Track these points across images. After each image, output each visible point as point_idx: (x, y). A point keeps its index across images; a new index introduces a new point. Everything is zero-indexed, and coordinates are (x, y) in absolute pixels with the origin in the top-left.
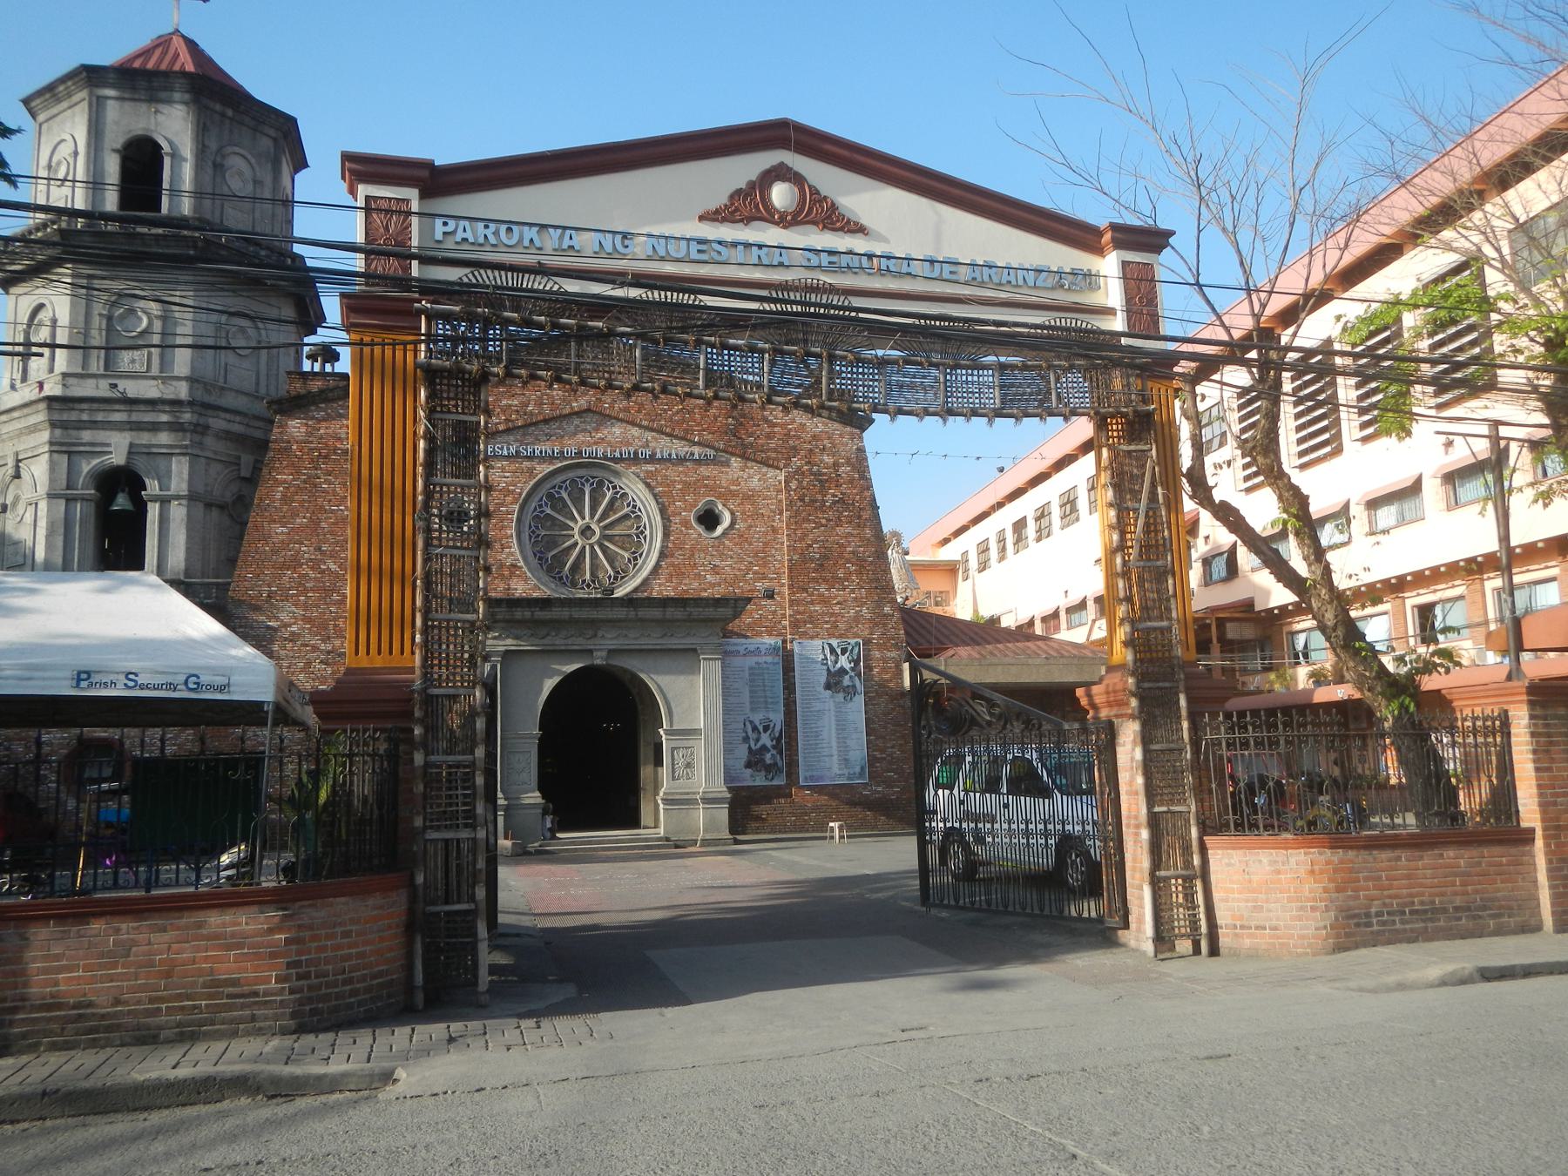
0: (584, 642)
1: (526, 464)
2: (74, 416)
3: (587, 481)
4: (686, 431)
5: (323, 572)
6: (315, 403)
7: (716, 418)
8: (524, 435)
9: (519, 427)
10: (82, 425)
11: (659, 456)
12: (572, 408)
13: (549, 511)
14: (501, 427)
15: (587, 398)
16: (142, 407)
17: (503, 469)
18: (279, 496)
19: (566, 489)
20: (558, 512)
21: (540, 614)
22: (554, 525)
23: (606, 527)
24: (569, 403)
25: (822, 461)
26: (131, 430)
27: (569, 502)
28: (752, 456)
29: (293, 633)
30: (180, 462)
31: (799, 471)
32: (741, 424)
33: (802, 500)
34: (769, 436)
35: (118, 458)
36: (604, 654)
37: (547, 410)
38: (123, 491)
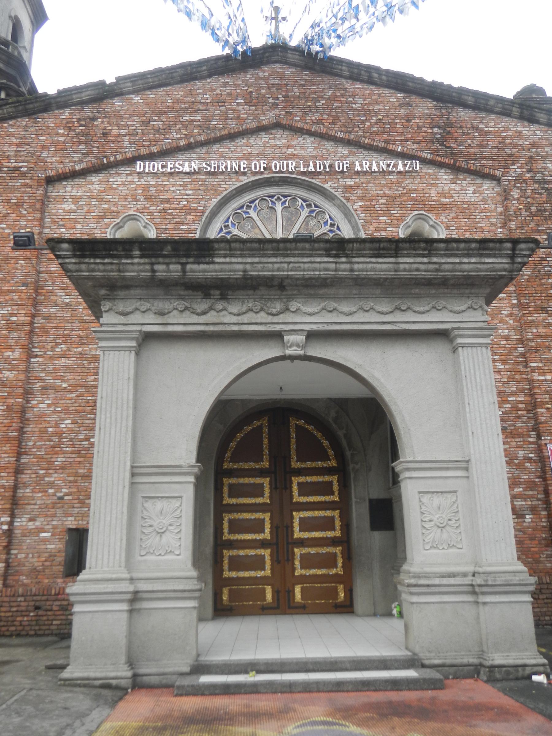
0: (270, 319)
1: (211, 180)
3: (279, 199)
4: (386, 141)
8: (207, 153)
11: (358, 168)
13: (235, 231)
14: (182, 143)
15: (277, 111)
17: (184, 186)
24: (256, 117)
25: (545, 168)
28: (464, 165)
31: (519, 180)
32: (449, 133)
33: (527, 208)
34: (482, 145)
36: (301, 338)
37: (233, 126)
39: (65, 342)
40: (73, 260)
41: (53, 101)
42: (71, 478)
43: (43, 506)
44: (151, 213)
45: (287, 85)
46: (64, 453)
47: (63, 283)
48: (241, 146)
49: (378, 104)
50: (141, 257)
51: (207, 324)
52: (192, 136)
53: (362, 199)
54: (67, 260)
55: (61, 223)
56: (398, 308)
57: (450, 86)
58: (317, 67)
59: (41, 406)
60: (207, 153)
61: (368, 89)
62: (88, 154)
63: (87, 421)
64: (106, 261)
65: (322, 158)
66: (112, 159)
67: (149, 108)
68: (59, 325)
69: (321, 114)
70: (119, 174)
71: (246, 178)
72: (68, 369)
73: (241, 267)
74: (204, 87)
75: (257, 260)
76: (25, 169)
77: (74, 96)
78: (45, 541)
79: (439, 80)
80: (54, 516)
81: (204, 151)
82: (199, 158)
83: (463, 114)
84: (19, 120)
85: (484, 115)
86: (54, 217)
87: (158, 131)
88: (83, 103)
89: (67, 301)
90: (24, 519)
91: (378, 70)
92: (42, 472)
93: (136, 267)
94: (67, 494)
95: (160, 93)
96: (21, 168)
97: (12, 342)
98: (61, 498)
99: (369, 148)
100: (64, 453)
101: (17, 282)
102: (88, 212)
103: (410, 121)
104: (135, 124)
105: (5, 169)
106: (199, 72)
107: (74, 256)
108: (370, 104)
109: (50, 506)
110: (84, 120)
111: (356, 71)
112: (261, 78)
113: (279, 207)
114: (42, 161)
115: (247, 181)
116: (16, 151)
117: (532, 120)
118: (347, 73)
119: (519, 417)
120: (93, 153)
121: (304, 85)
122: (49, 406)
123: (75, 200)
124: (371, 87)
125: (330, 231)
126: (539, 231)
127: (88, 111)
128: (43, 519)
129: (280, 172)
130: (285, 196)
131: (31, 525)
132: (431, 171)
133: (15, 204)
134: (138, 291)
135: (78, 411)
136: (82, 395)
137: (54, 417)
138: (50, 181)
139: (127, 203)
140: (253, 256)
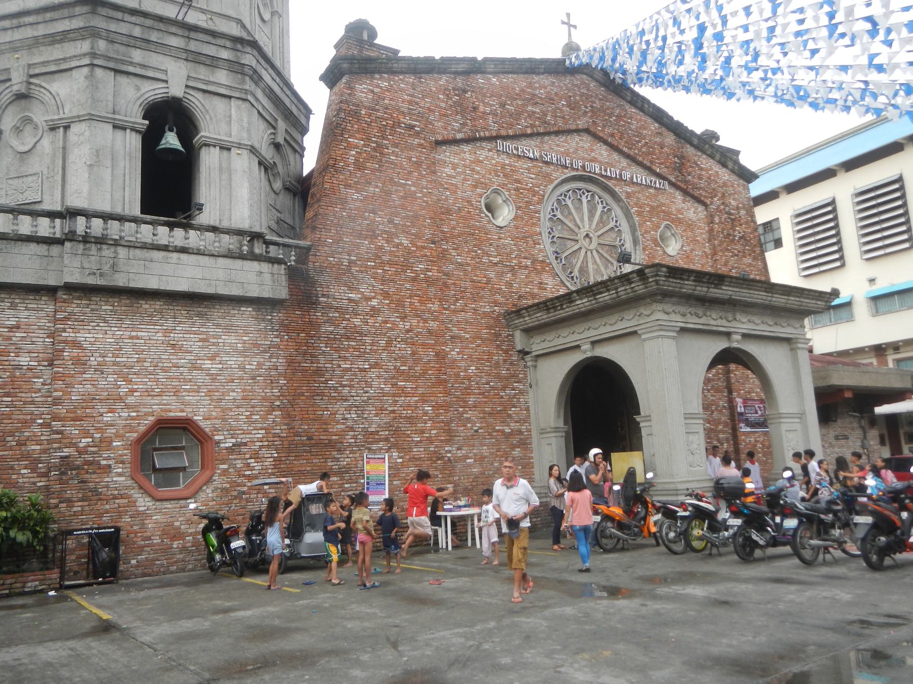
1: (545, 169)
2: (124, 28)
5: (397, 246)
6: (380, 72)
7: (668, 155)
8: (542, 142)
9: (539, 134)
10: (132, 42)
12: (577, 125)
13: (559, 216)
14: (529, 131)
16: (201, 36)
18: (352, 160)
19: (570, 198)
20: (566, 217)
21: (715, 292)
22: (562, 229)
23: (599, 237)
25: (730, 203)
26: (186, 60)
27: (573, 211)
29: (373, 308)
30: (239, 108)
32: (683, 164)
33: (722, 233)
35: (176, 90)
37: (560, 123)
38: (171, 130)
39: (462, 298)
40: (664, 279)
41: (437, 66)
42: (481, 415)
43: (465, 438)
44: (509, 190)
45: (592, 96)
46: (474, 394)
47: (454, 244)
48: (563, 142)
49: (645, 129)
50: (694, 281)
51: (703, 324)
52: (535, 126)
53: (636, 204)
54: (662, 278)
55: (445, 186)
56: (776, 324)
57: (686, 128)
58: (611, 87)
59: (452, 353)
60: (542, 142)
61: (640, 115)
62: (464, 125)
63: (486, 368)
64: (678, 281)
65: (612, 166)
66: (482, 134)
67: (504, 91)
68: (457, 282)
69: (614, 129)
70: (483, 148)
71: (567, 171)
72: (467, 322)
73: (730, 293)
74: (538, 82)
75: (737, 290)
76: (418, 129)
77: (453, 66)
78: (470, 465)
79: (682, 121)
80: (473, 446)
81: (539, 140)
82: (536, 146)
83: (690, 150)
84: (407, 76)
85: (699, 154)
86: (440, 180)
87: (511, 115)
88: (457, 73)
89: (460, 261)
90: (454, 449)
91: (648, 102)
92: (461, 409)
93: (689, 287)
94: (480, 428)
95: (510, 80)
96: (415, 126)
97: (431, 295)
98: (476, 431)
99: (640, 164)
100: (474, 394)
101: (427, 239)
102: (465, 179)
103: (662, 148)
104: (494, 102)
105: (403, 125)
106: (539, 68)
107: (665, 276)
108: (640, 128)
109: (470, 437)
110: (458, 90)
111: (635, 99)
112: (576, 86)
113: (584, 200)
114: (431, 123)
115: (569, 175)
116: (409, 109)
117: (724, 165)
118: (629, 98)
119: (719, 379)
120: (468, 126)
121: (602, 100)
122: (458, 353)
123: (454, 169)
124: (641, 113)
125: (615, 226)
126: (728, 250)
127: (460, 81)
128: (466, 448)
129: (590, 172)
130: (588, 191)
131: (460, 453)
132: (672, 191)
133: (416, 163)
134: (674, 299)
135: (479, 359)
136: (478, 346)
137: (463, 364)
138: (439, 143)
139: (491, 177)
140: (737, 287)
